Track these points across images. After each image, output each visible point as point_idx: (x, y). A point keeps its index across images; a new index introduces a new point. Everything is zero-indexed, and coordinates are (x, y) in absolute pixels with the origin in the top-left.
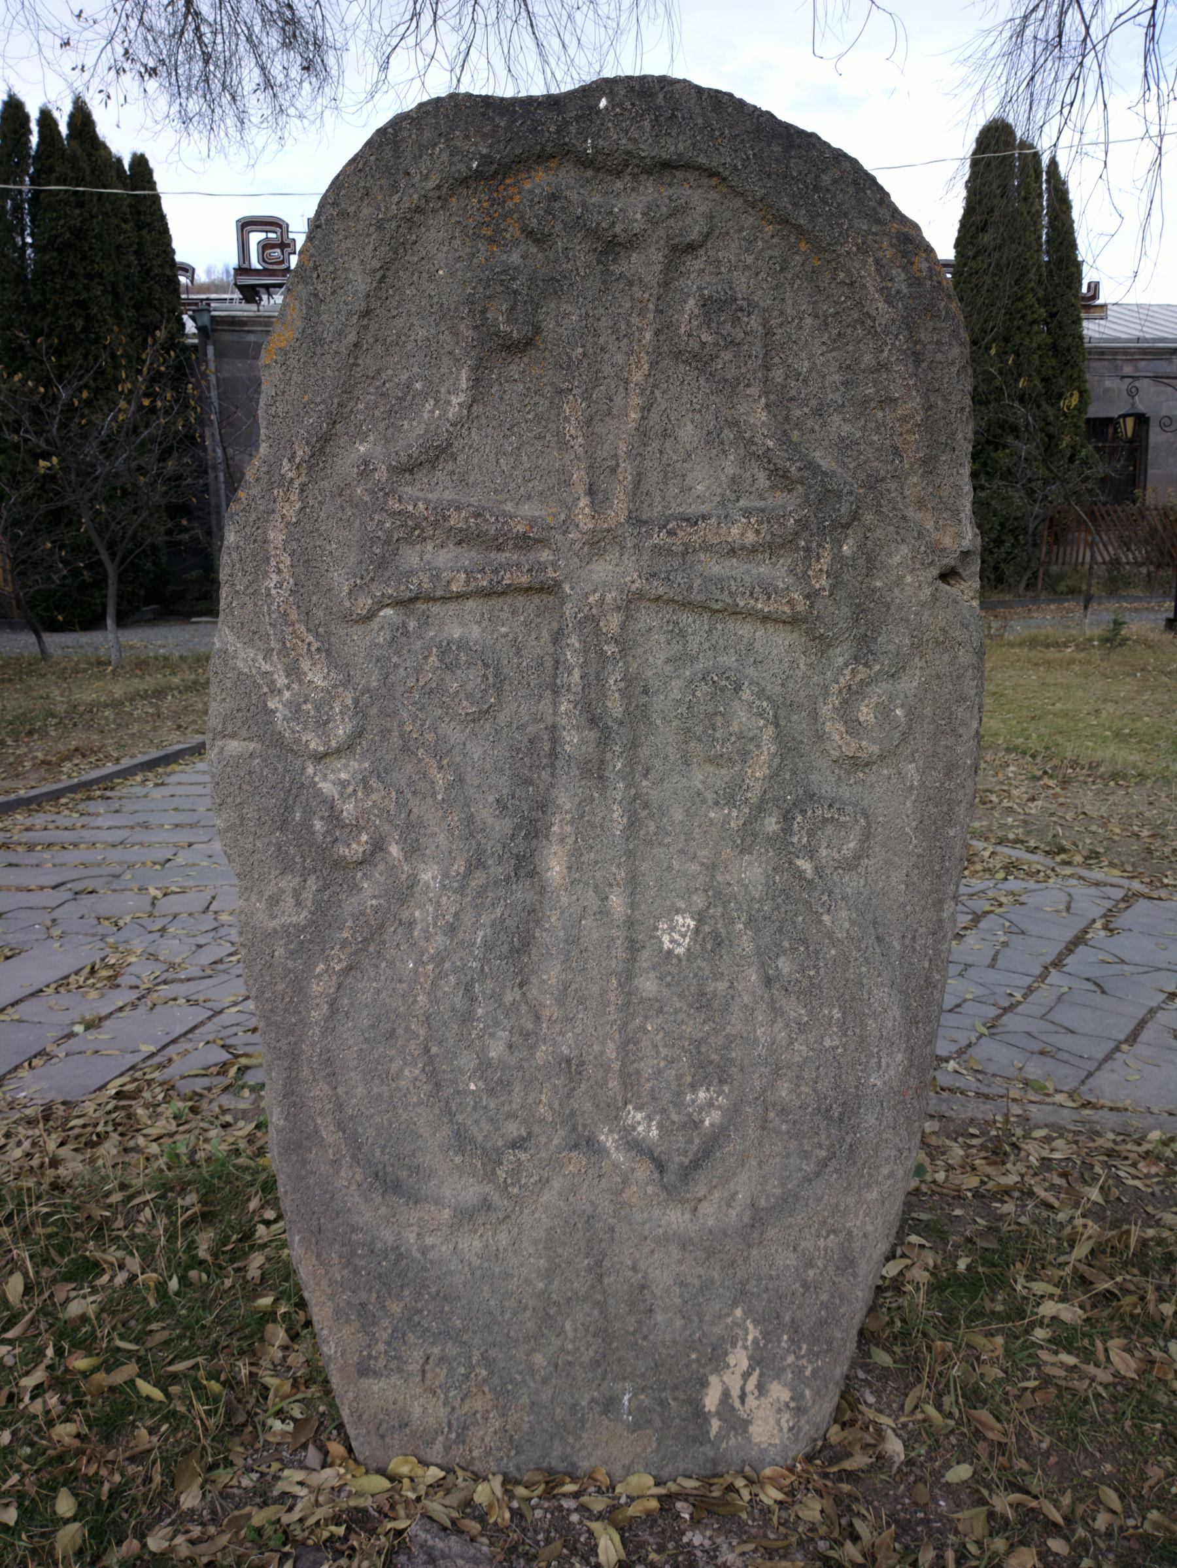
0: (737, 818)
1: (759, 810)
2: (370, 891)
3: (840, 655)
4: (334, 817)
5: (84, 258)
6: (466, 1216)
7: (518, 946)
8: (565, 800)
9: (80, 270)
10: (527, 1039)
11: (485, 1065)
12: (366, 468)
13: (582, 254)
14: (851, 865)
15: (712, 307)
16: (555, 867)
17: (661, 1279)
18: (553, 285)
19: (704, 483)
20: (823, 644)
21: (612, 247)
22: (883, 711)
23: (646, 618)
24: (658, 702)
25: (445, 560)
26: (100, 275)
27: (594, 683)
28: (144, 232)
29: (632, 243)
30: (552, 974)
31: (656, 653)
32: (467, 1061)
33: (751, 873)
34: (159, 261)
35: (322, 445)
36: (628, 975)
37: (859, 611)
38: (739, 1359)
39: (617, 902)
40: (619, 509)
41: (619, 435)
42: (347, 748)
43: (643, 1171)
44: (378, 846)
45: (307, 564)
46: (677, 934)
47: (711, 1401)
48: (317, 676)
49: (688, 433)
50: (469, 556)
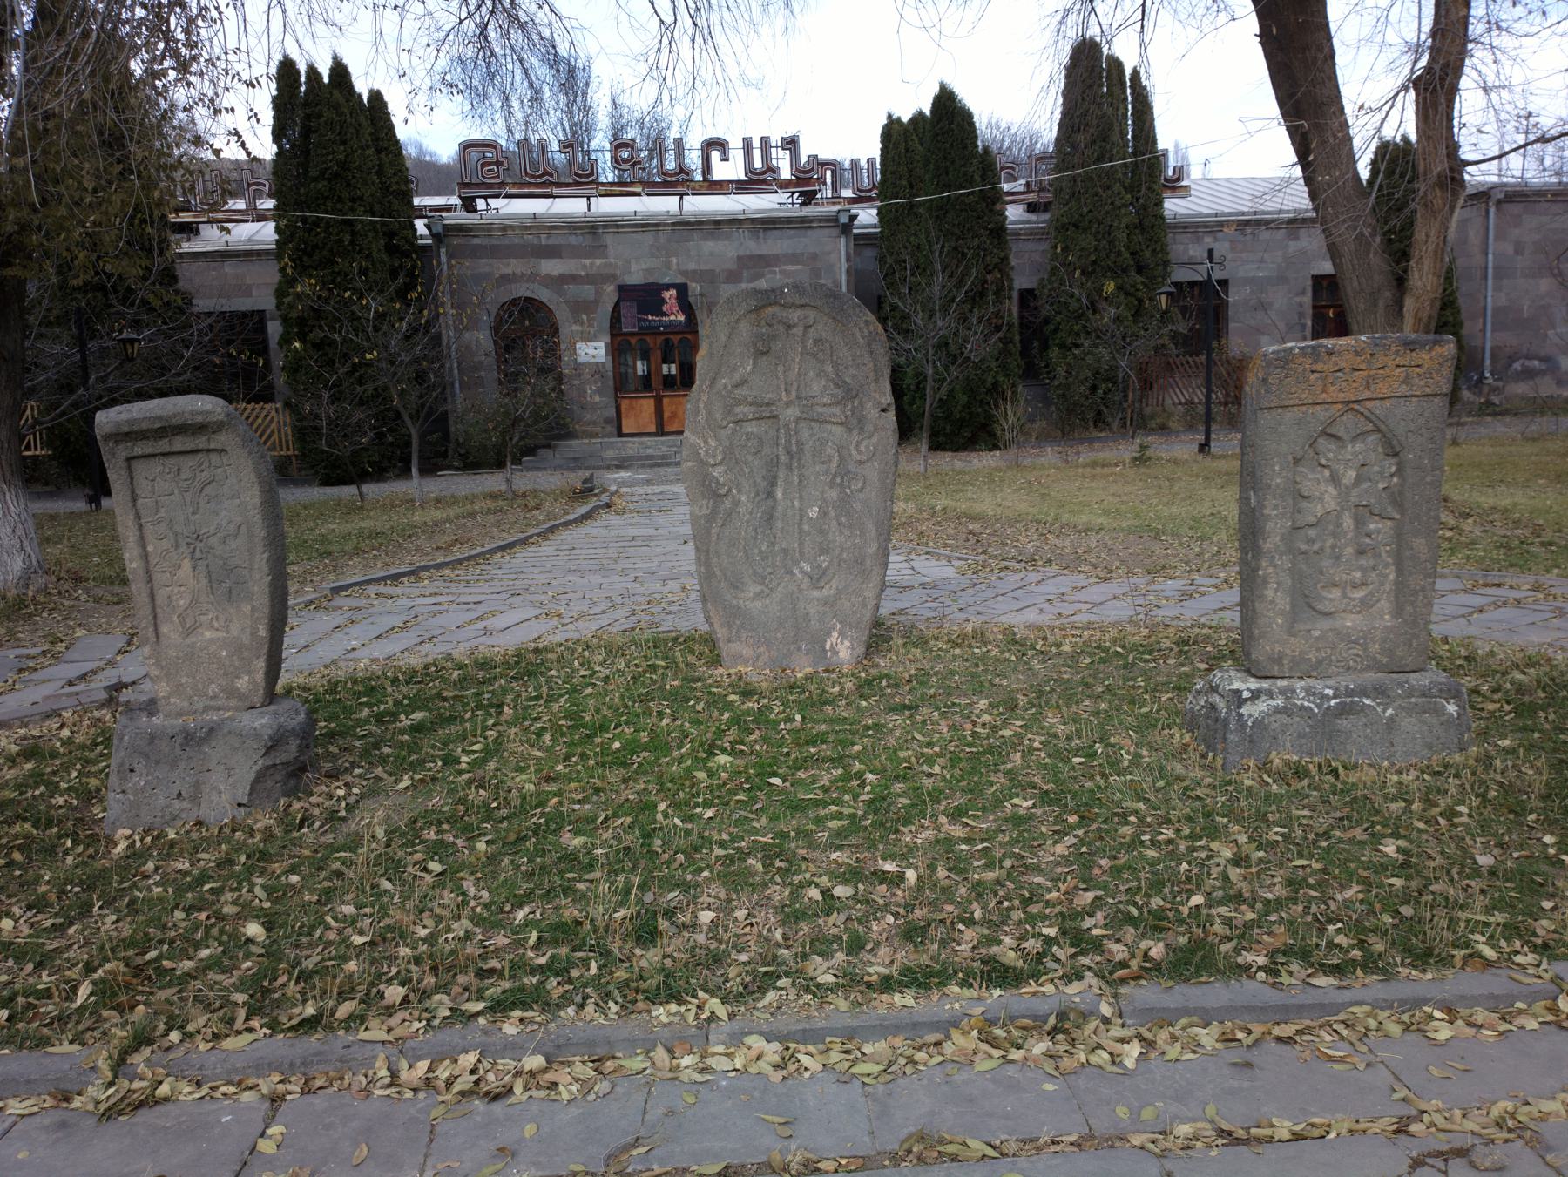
0: (829, 478)
1: (835, 476)
2: (727, 503)
3: (855, 433)
4: (718, 482)
5: (348, 185)
6: (757, 596)
7: (769, 518)
8: (781, 475)
9: (345, 195)
10: (773, 544)
11: (761, 552)
12: (725, 386)
13: (782, 330)
14: (861, 490)
15: (816, 341)
16: (779, 495)
17: (812, 611)
18: (774, 337)
19: (816, 388)
20: (851, 430)
21: (789, 327)
22: (867, 448)
23: (802, 424)
24: (806, 447)
25: (745, 410)
26: (361, 199)
27: (788, 442)
28: (383, 155)
29: (795, 326)
30: (779, 524)
31: (805, 434)
32: (756, 551)
33: (833, 494)
34: (395, 179)
35: (713, 381)
36: (800, 524)
37: (860, 421)
38: (835, 634)
39: (796, 503)
40: (793, 395)
41: (793, 375)
43: (807, 579)
44: (730, 490)
45: (709, 413)
46: (813, 512)
47: (828, 647)
48: (712, 443)
49: (811, 374)
50: (753, 409)
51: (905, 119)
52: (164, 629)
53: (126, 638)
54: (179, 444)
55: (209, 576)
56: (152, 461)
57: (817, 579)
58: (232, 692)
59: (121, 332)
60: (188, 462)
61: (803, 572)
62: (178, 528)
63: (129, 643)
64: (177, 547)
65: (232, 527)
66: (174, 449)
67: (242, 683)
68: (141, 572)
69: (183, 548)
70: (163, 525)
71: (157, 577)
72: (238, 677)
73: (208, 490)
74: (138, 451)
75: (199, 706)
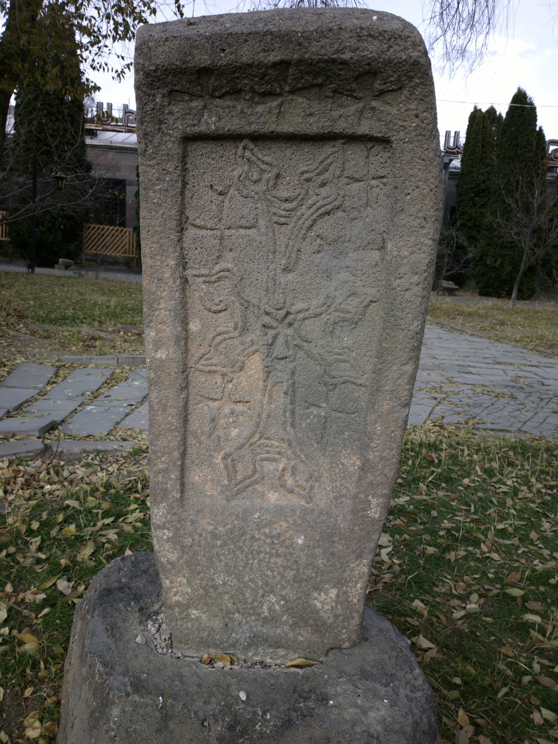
51: (484, 110)
52: (196, 476)
53: (54, 370)
54: (299, 114)
55: (292, 392)
56: (230, 150)
59: (57, 173)
60: (299, 161)
62: (251, 295)
63: (56, 375)
64: (244, 330)
65: (353, 304)
66: (286, 128)
67: (325, 601)
68: (174, 369)
69: (255, 334)
70: (226, 284)
71: (198, 379)
72: (318, 588)
73: (325, 226)
74: (210, 123)
75: (241, 635)
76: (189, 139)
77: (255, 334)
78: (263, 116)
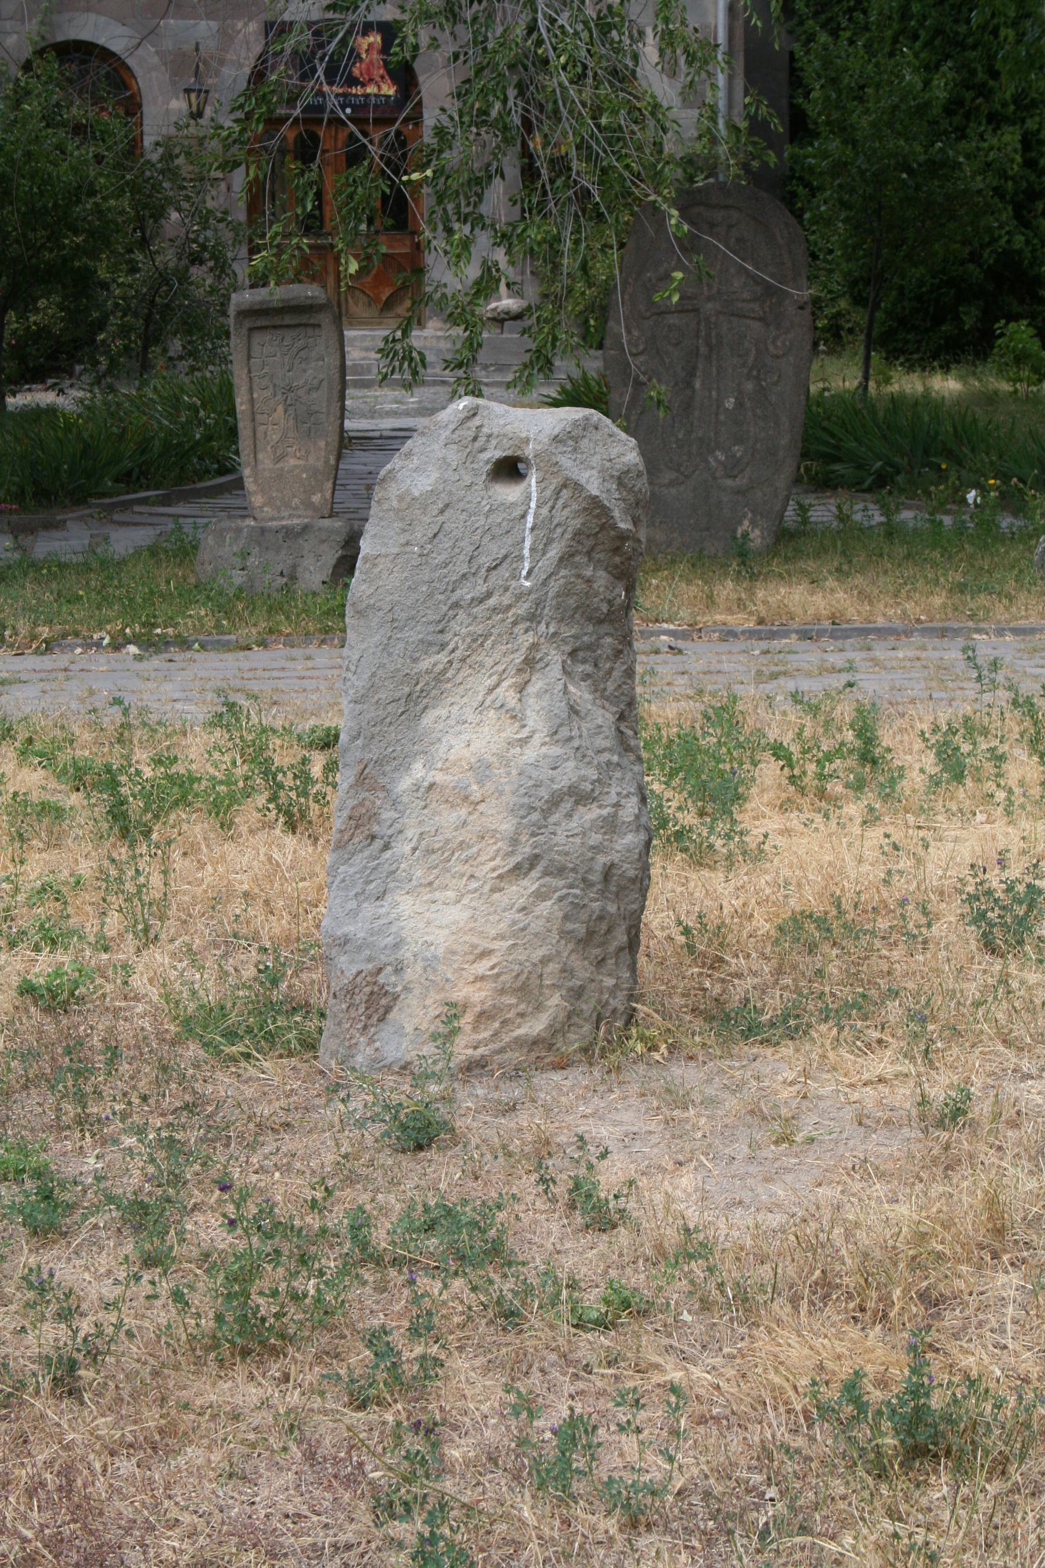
0: (745, 371)
1: (751, 369)
6: (672, 484)
8: (700, 366)
14: (776, 384)
16: (698, 385)
20: (768, 325)
30: (697, 413)
33: (749, 386)
38: (746, 523)
42: (642, 353)
46: (730, 403)
48: (636, 333)
52: (260, 456)
54: (288, 320)
55: (296, 418)
57: (733, 468)
58: (308, 505)
61: (716, 460)
69: (279, 397)
71: (258, 417)
74: (259, 323)
76: (251, 330)
77: (279, 397)
78: (277, 321)
